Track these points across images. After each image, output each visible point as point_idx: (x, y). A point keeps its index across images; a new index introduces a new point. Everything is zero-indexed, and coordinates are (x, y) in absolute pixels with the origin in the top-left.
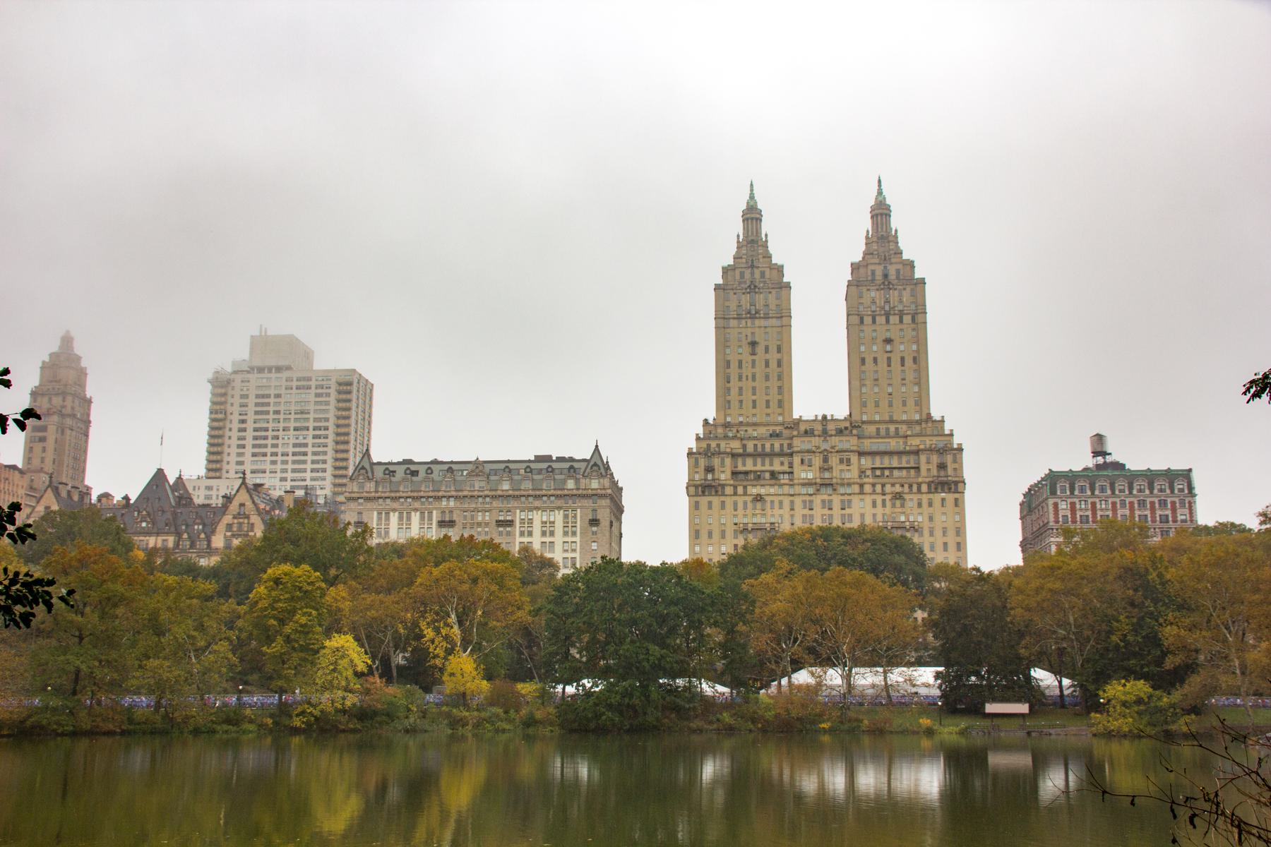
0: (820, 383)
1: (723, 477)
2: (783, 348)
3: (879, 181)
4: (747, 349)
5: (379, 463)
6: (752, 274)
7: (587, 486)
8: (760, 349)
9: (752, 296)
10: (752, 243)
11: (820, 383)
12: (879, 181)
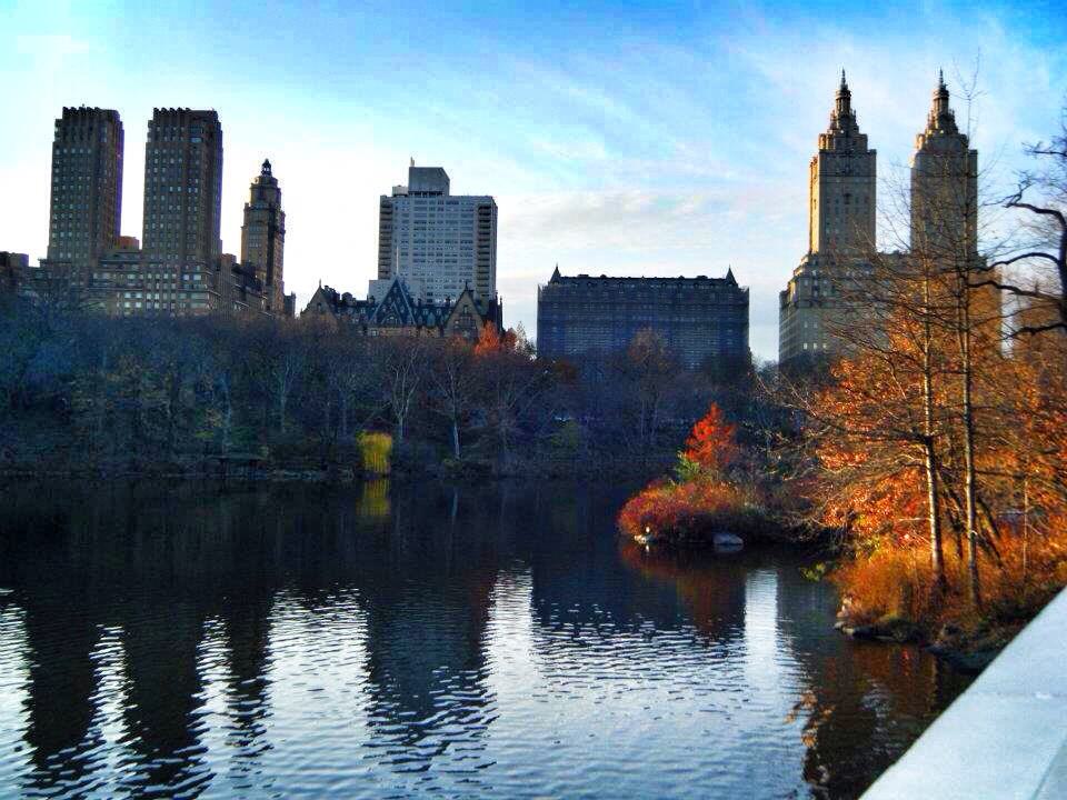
0: (893, 231)
1: (825, 294)
2: (869, 202)
3: (941, 72)
4: (842, 200)
5: (566, 278)
6: (847, 142)
7: (721, 301)
8: (852, 200)
9: (845, 157)
10: (845, 116)
11: (893, 231)
12: (941, 72)
